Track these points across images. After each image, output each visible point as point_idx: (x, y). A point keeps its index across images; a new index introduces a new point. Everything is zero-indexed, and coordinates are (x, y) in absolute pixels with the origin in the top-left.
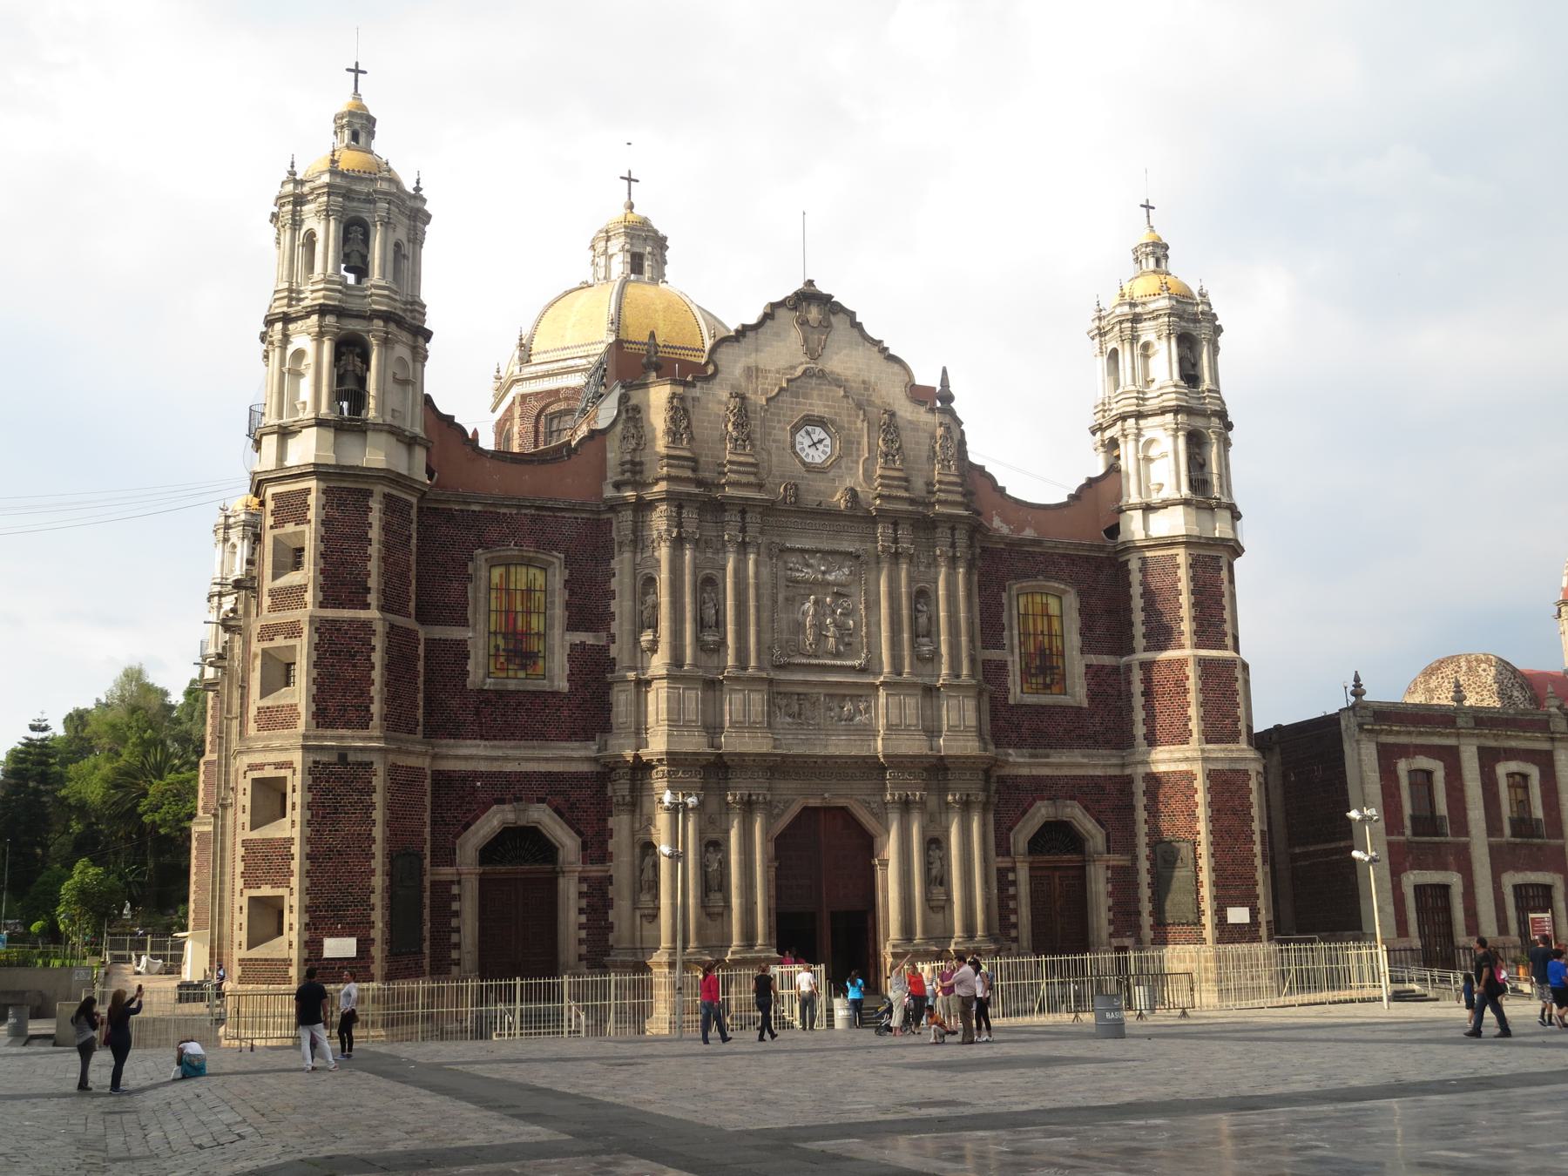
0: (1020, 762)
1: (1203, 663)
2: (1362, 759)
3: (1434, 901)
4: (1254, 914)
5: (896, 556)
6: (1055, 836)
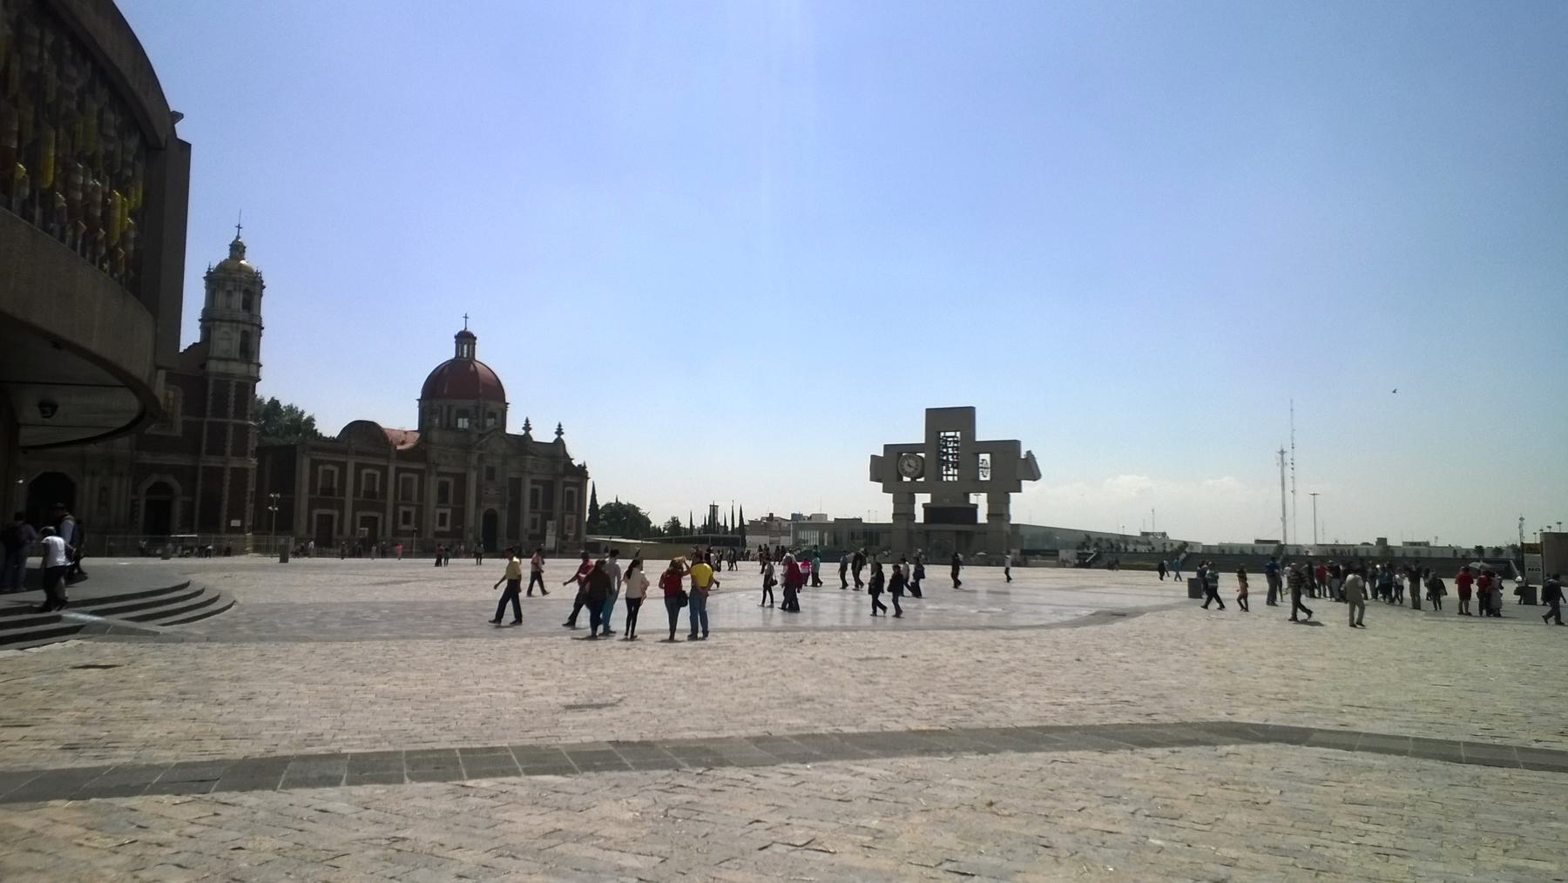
0: (147, 458)
1: (236, 426)
2: (304, 466)
3: (326, 522)
4: (243, 523)
6: (161, 487)
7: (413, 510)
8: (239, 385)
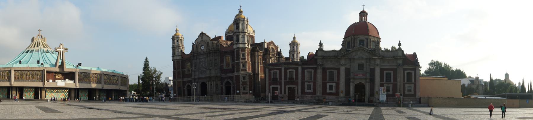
0: (224, 75)
1: (236, 62)
4: (240, 91)
5: (208, 57)
6: (228, 83)
7: (312, 84)
8: (237, 51)
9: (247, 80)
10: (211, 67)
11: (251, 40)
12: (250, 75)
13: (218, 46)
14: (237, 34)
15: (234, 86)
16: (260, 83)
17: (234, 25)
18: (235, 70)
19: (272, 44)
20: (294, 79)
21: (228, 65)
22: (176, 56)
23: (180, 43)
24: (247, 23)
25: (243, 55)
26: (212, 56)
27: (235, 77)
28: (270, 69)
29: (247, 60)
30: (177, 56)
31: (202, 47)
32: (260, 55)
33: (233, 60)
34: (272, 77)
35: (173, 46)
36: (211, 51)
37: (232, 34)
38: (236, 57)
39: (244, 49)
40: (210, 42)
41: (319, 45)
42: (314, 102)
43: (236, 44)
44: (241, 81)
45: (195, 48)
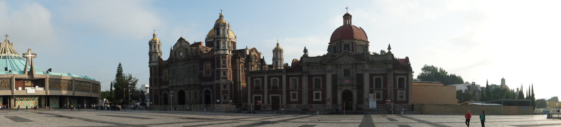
0: (203, 83)
1: (216, 70)
4: (220, 100)
6: (207, 91)
7: (297, 93)
8: (217, 57)
9: (228, 88)
10: (190, 74)
11: (232, 46)
12: (231, 84)
13: (198, 52)
14: (218, 40)
15: (214, 95)
16: (242, 92)
17: (214, 30)
18: (215, 78)
19: (254, 51)
20: (278, 88)
21: (208, 72)
22: (152, 62)
23: (157, 49)
24: (229, 28)
25: (224, 62)
26: (191, 63)
27: (215, 85)
28: (252, 77)
29: (228, 67)
30: (154, 62)
31: (180, 54)
32: (242, 62)
33: (213, 67)
34: (255, 86)
35: (150, 51)
36: (190, 57)
37: (212, 40)
38: (216, 64)
39: (224, 56)
40: (189, 48)
41: (304, 52)
42: (299, 112)
43: (217, 50)
44: (221, 90)
45: (173, 54)
